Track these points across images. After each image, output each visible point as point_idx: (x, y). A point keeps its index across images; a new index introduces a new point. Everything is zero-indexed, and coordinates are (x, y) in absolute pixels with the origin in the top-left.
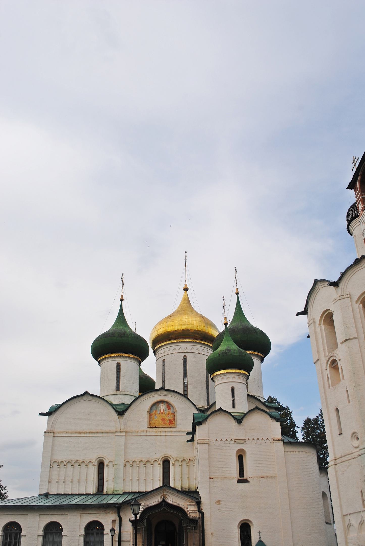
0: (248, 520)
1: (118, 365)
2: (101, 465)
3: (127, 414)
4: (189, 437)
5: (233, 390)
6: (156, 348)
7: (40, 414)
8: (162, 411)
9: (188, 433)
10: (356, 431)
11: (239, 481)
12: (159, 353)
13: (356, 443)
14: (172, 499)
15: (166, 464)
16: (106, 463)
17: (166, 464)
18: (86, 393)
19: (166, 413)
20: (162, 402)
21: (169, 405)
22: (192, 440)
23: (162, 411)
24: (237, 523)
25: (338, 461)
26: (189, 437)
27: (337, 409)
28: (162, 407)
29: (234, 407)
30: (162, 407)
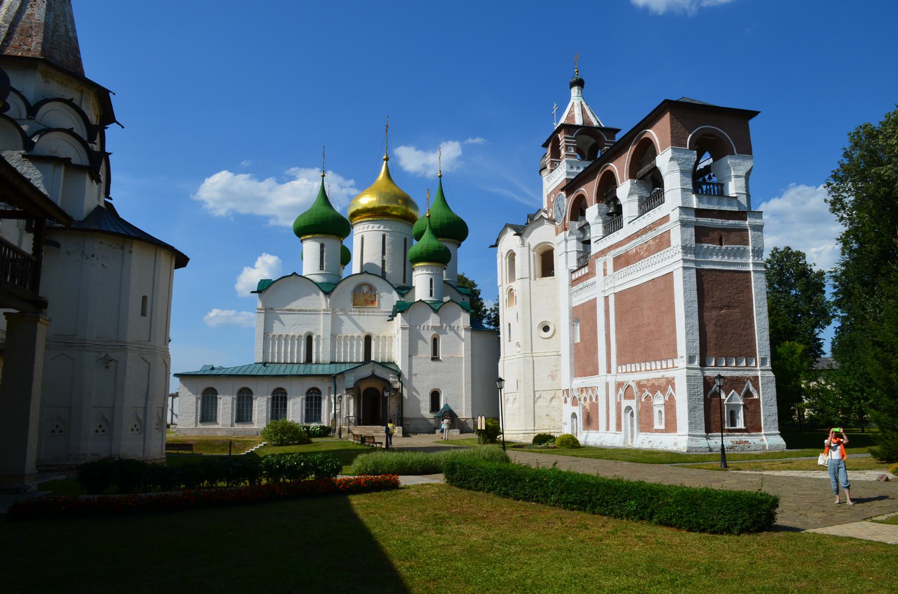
0: (439, 389)
1: (322, 246)
2: (309, 339)
3: (334, 294)
4: (390, 318)
5: (431, 280)
6: (355, 222)
7: (251, 292)
8: (365, 292)
9: (390, 316)
10: (519, 341)
11: (433, 359)
12: (358, 227)
13: (518, 349)
14: (380, 372)
15: (368, 339)
16: (314, 337)
17: (368, 339)
18: (295, 273)
19: (369, 294)
20: (365, 284)
21: (371, 288)
22: (392, 320)
23: (365, 292)
24: (429, 391)
25: (505, 359)
26: (390, 318)
27: (509, 324)
28: (365, 289)
29: (431, 295)
30: (365, 289)
